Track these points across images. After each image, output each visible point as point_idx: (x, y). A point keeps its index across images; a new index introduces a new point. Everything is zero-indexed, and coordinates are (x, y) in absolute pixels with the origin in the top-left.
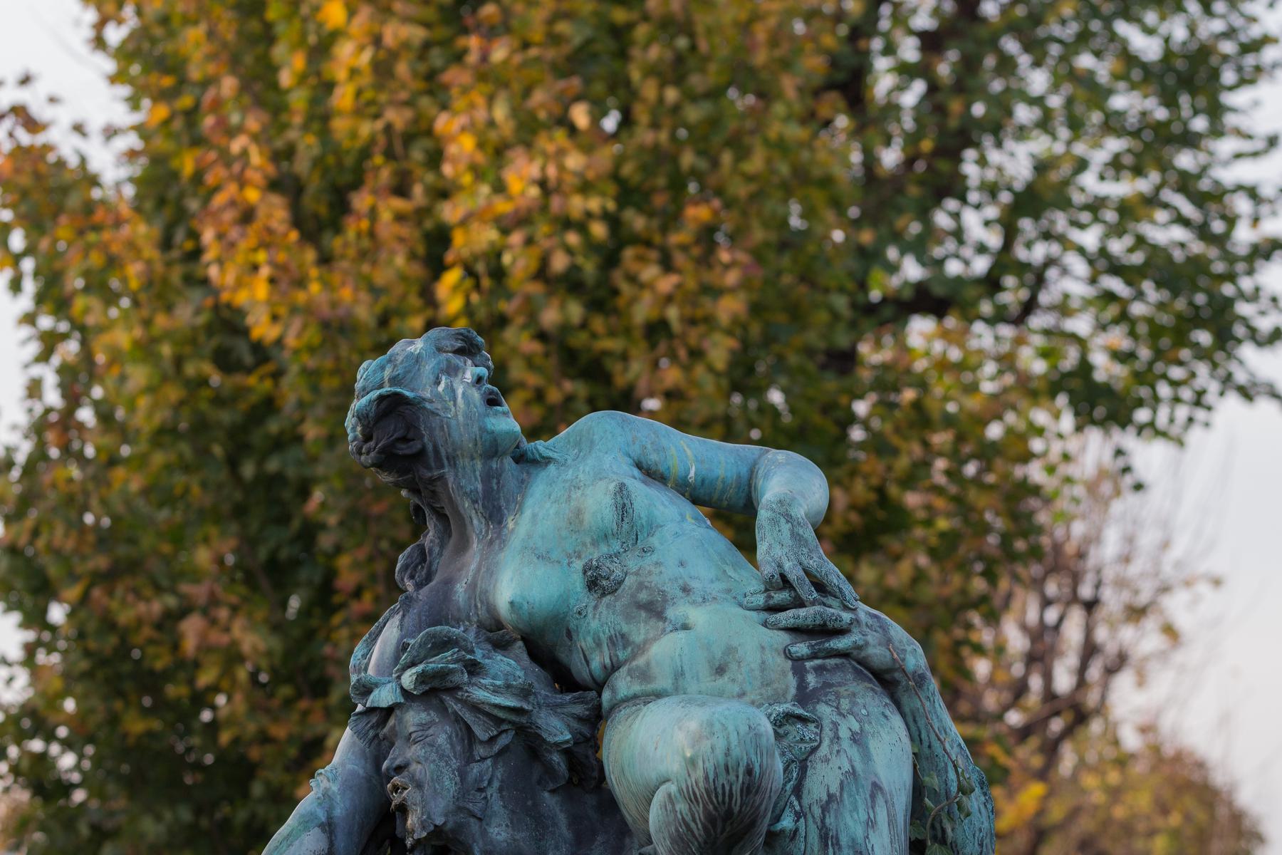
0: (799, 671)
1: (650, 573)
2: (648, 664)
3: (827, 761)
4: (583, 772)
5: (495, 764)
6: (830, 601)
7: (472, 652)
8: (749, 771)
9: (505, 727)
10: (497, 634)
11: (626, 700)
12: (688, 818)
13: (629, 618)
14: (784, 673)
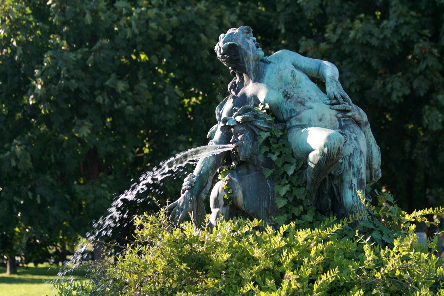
2: (301, 118)
3: (349, 145)
6: (346, 103)
8: (339, 149)
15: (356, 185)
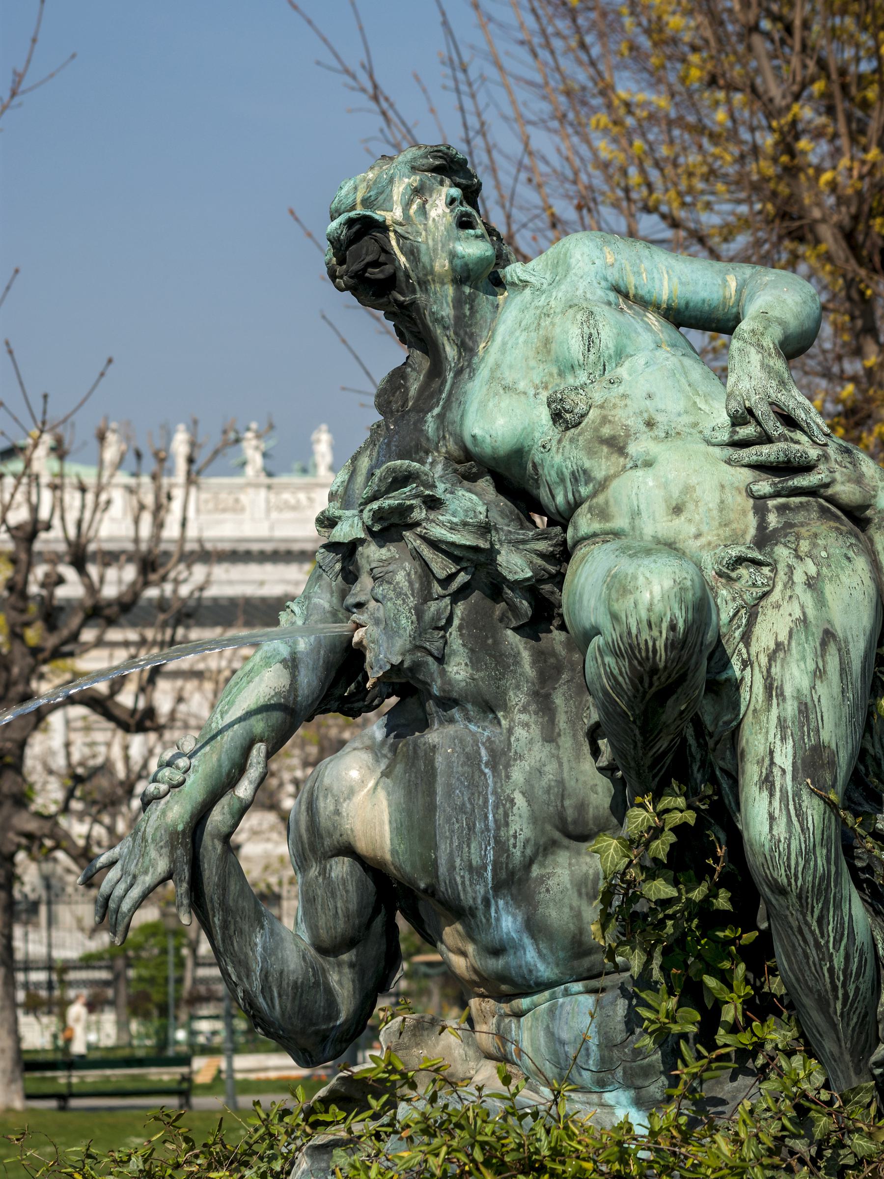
0: (761, 511)
1: (615, 406)
2: (607, 502)
3: (778, 607)
4: (542, 609)
5: (454, 602)
6: (799, 435)
7: (433, 486)
9: (465, 565)
10: (471, 464)
11: (584, 539)
12: (616, 672)
13: (591, 453)
14: (744, 513)
15: (789, 769)
